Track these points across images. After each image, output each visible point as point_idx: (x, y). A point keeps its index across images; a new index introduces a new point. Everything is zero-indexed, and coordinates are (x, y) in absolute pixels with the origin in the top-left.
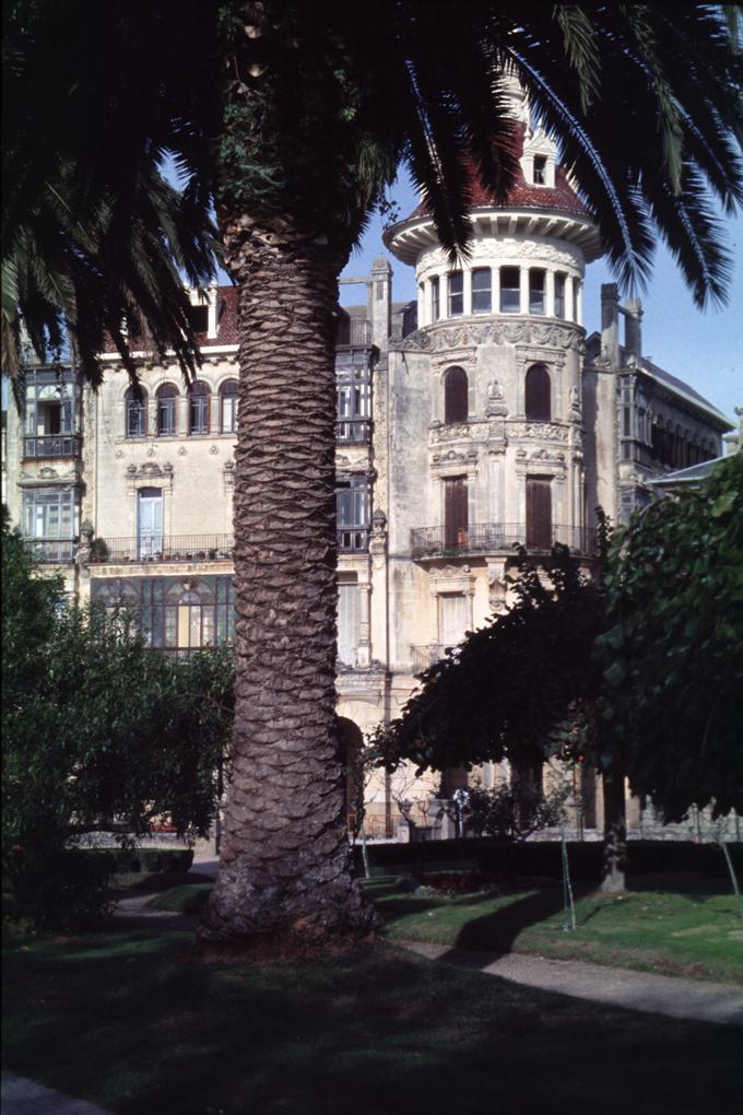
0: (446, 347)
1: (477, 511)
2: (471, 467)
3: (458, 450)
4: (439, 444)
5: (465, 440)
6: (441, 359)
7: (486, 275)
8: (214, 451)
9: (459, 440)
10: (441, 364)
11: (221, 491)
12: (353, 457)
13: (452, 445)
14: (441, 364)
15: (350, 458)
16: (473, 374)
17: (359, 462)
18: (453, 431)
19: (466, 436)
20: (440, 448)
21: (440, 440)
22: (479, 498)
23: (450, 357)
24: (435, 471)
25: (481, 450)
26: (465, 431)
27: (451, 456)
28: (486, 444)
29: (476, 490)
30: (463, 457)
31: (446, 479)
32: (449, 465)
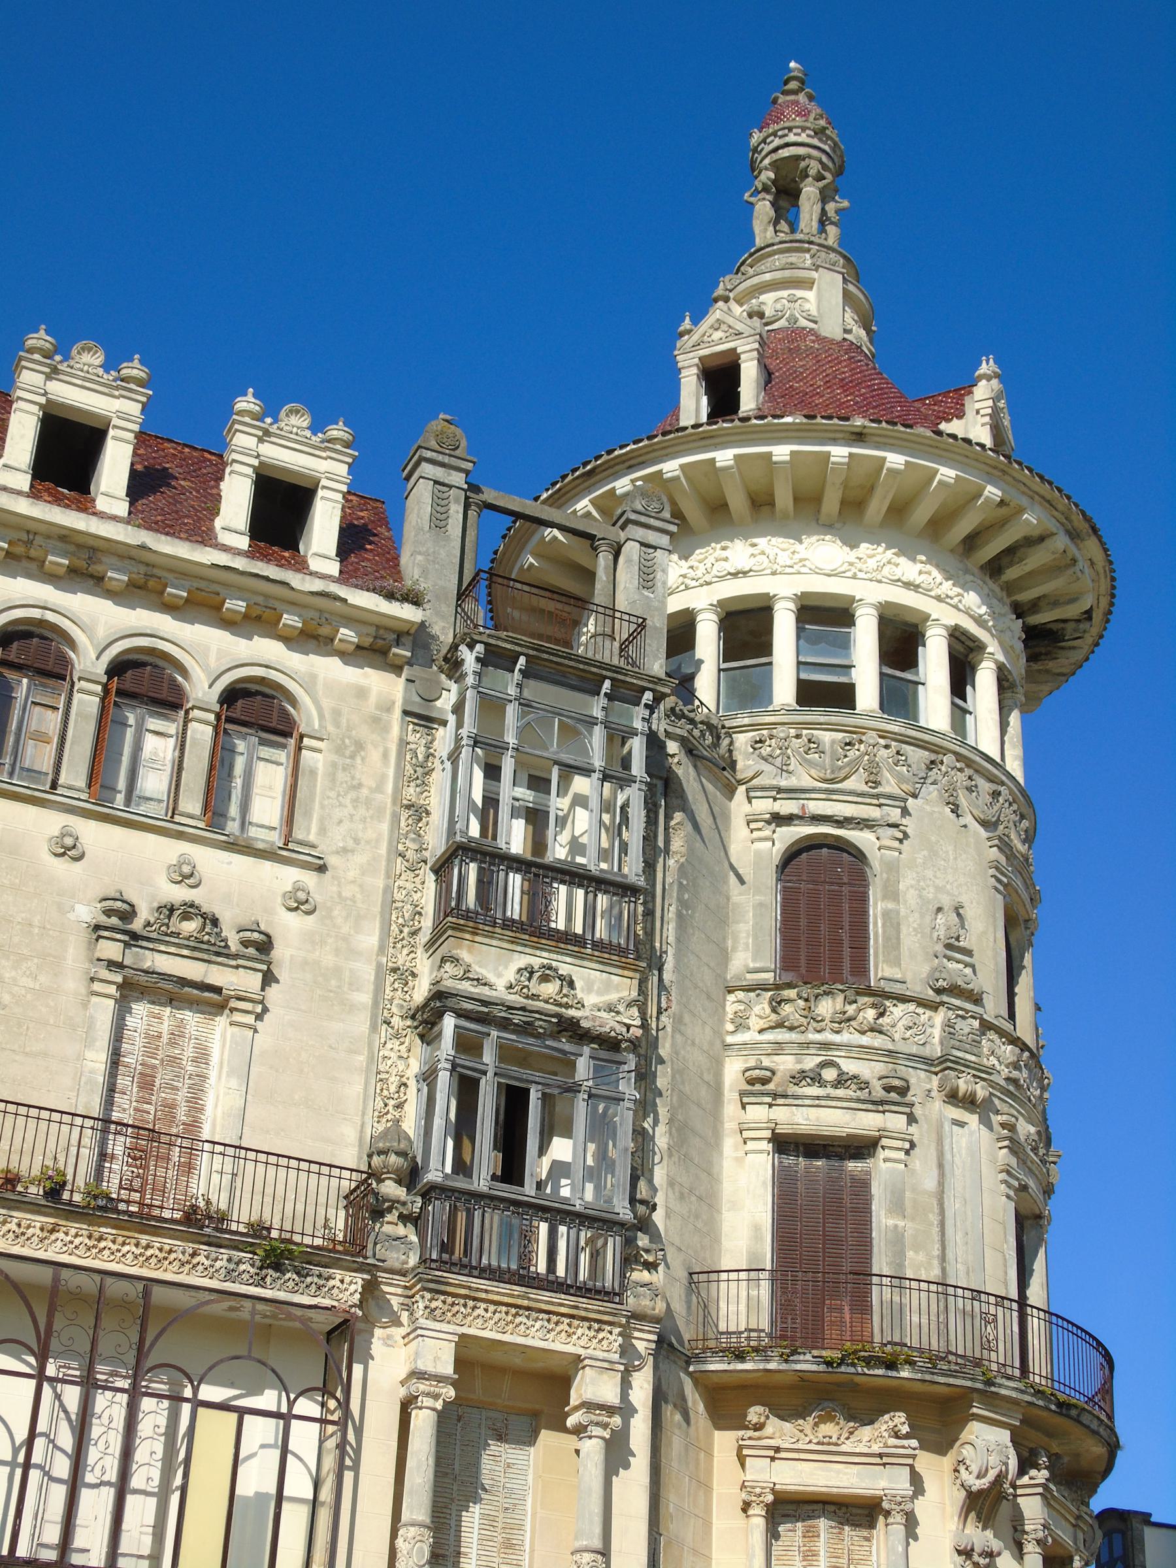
0: (803, 778)
1: (910, 1254)
2: (896, 1122)
3: (850, 1066)
4: (769, 1036)
5: (878, 1041)
6: (787, 807)
7: (768, 667)
8: (68, 850)
9: (845, 1037)
10: (778, 819)
11: (73, 984)
12: (589, 989)
13: (826, 1046)
14: (778, 819)
15: (578, 984)
16: (893, 868)
17: (611, 1009)
18: (826, 1007)
19: (876, 1030)
20: (778, 1048)
21: (780, 1025)
22: (913, 1219)
23: (817, 807)
24: (758, 1113)
25: (921, 1082)
26: (871, 1014)
27: (829, 1074)
28: (942, 1064)
29: (908, 1194)
30: (864, 1085)
31: (783, 1144)
32: (818, 1102)
